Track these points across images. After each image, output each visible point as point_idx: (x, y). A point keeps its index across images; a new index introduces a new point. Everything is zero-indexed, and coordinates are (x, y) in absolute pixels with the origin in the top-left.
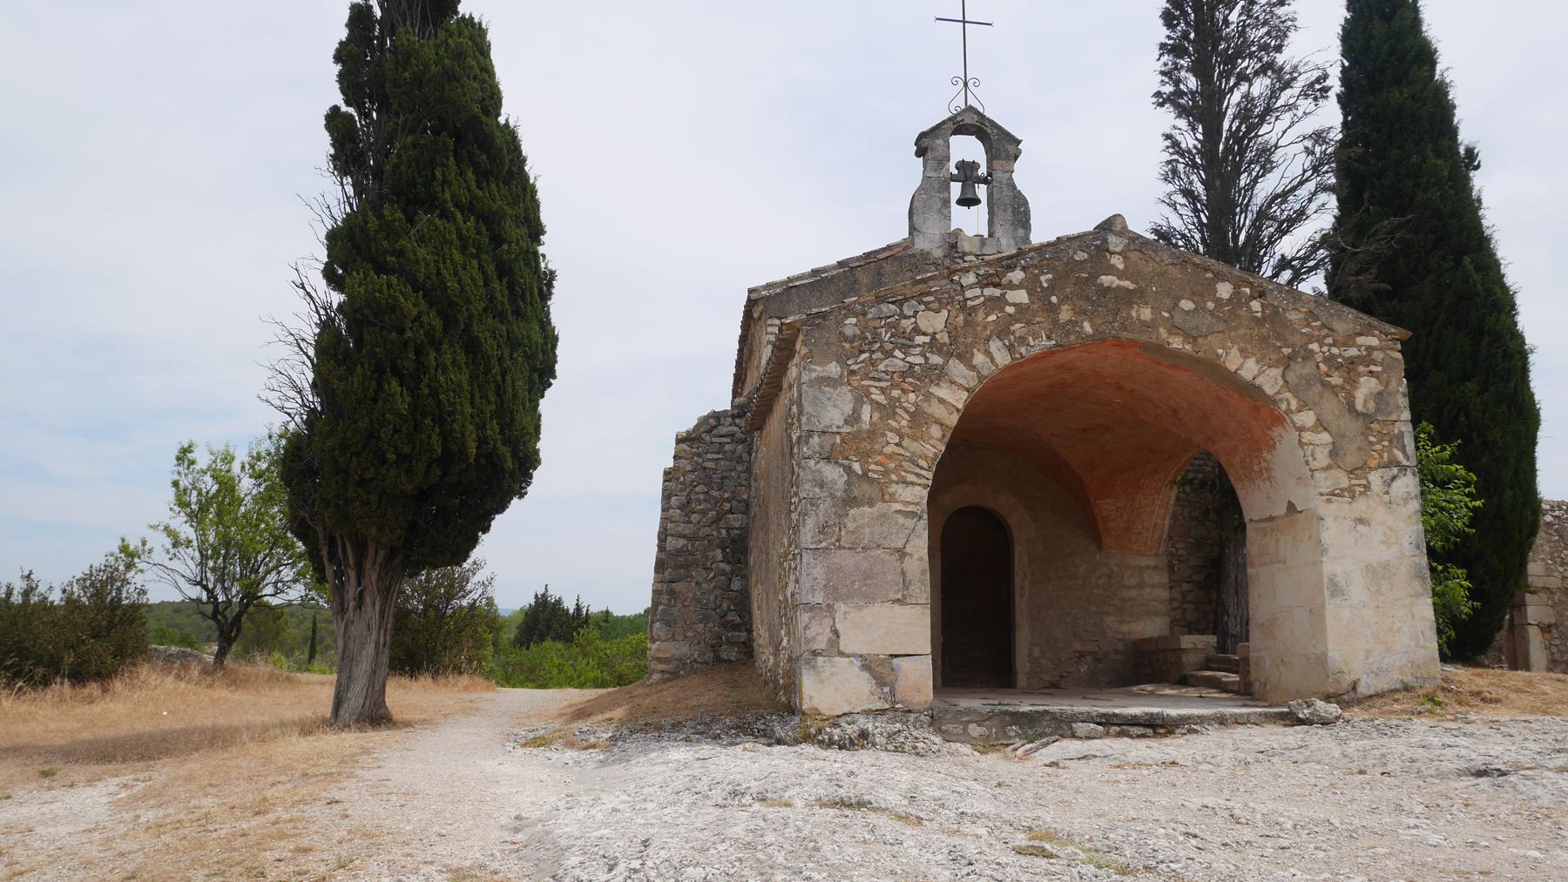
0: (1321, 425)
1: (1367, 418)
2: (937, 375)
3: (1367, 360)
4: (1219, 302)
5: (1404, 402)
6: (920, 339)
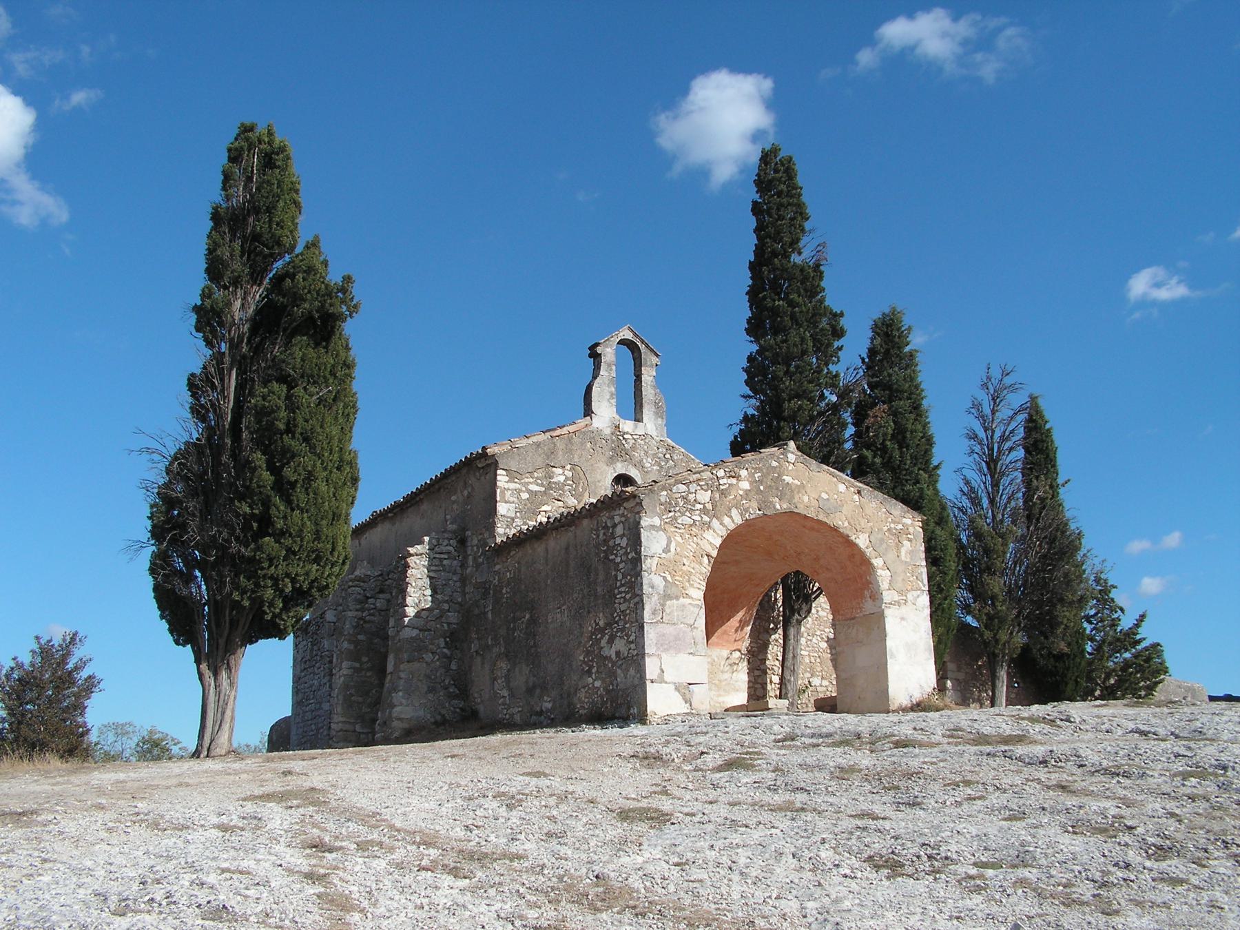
6: (699, 506)
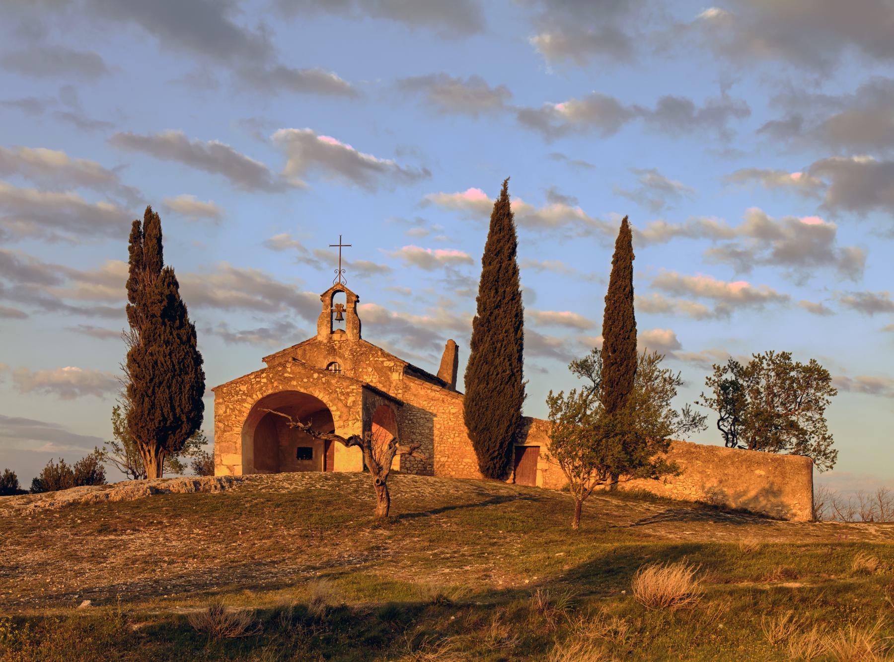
0: (338, 410)
1: (350, 408)
2: (244, 401)
3: (352, 392)
4: (314, 379)
5: (360, 403)
